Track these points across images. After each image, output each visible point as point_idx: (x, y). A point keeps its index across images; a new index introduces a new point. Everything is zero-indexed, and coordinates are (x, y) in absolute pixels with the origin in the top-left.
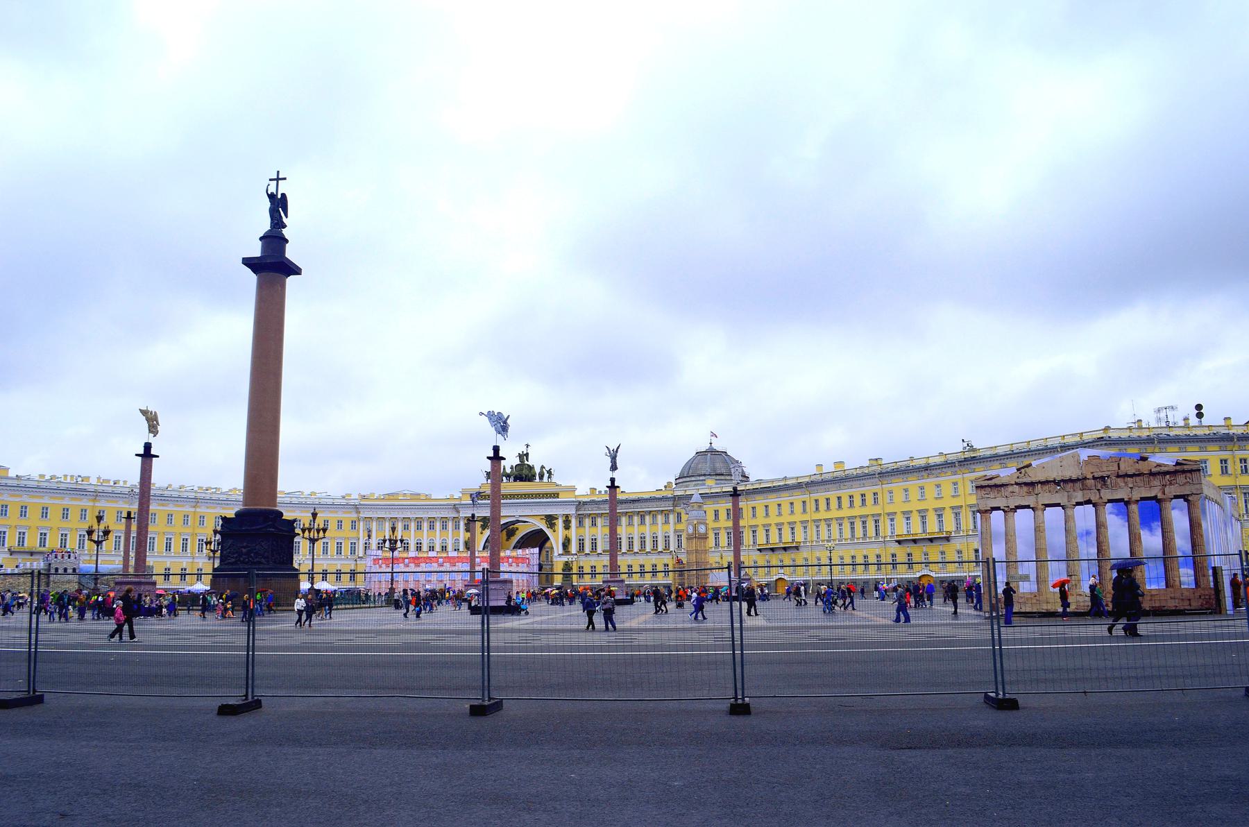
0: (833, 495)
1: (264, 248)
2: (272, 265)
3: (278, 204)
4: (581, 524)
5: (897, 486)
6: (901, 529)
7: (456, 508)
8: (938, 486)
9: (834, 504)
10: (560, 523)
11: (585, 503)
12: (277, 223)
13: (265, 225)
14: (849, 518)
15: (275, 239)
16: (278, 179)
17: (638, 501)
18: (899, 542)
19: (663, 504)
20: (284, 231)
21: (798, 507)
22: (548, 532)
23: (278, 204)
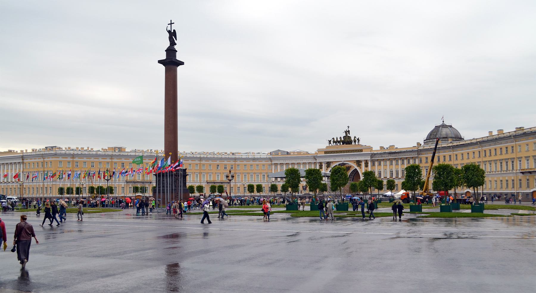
0: (492, 147)
1: (167, 55)
2: (171, 62)
3: (172, 35)
4: (374, 165)
5: (523, 142)
6: (525, 166)
7: (315, 158)
8: (527, 145)
9: (493, 152)
10: (363, 164)
11: (375, 154)
12: (173, 43)
13: (168, 44)
14: (500, 160)
15: (171, 51)
16: (171, 24)
17: (401, 152)
18: (523, 173)
19: (413, 153)
20: (175, 47)
21: (477, 154)
22: (358, 169)
23: (172, 35)
